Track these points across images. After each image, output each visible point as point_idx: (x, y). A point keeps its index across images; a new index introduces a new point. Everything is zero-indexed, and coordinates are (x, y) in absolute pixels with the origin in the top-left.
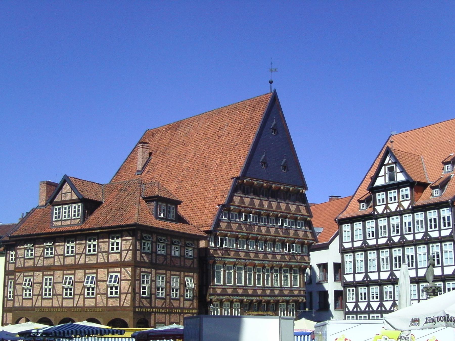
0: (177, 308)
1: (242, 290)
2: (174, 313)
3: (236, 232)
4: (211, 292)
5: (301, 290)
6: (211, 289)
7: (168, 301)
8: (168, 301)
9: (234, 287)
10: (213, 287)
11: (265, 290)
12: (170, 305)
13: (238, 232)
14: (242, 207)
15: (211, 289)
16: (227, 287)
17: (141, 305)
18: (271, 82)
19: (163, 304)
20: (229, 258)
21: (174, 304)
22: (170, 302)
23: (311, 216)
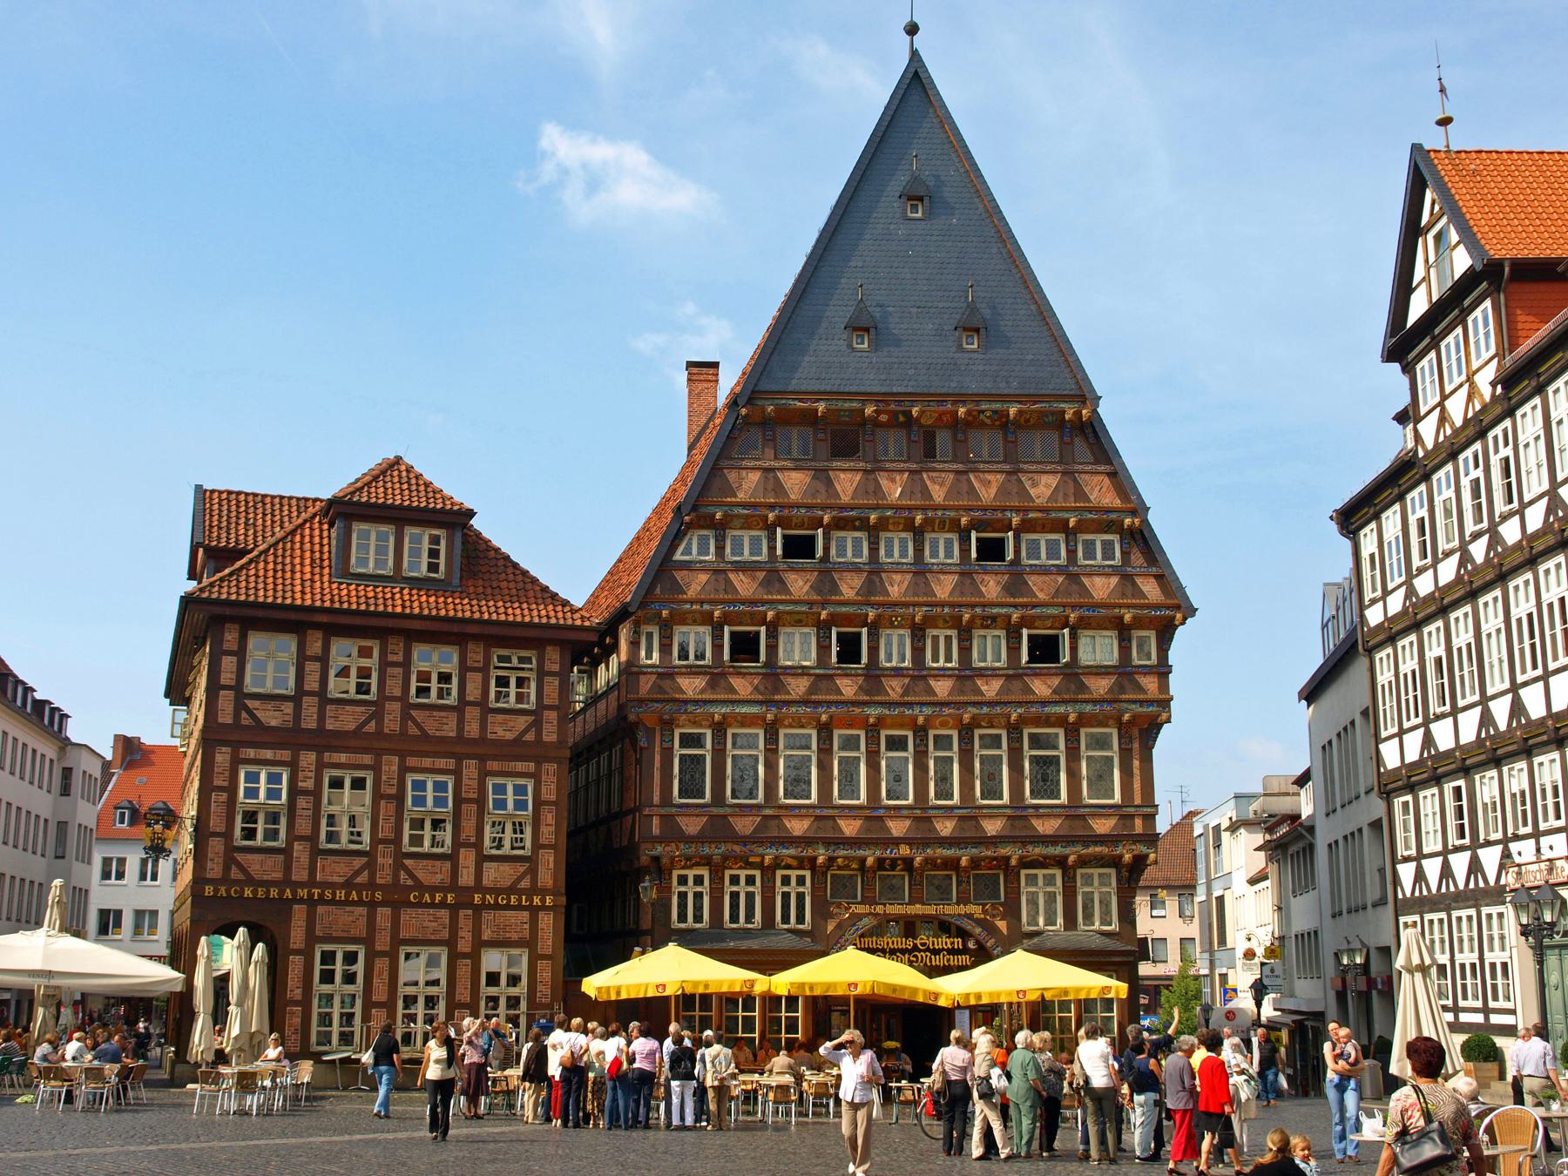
0: (433, 889)
1: (806, 823)
2: (420, 904)
3: (753, 602)
4: (656, 831)
5: (1132, 817)
6: (656, 821)
7: (385, 860)
8: (385, 860)
9: (768, 812)
10: (663, 811)
11: (929, 819)
12: (396, 876)
13: (764, 603)
14: (772, 507)
15: (656, 821)
16: (728, 810)
17: (235, 873)
18: (912, 29)
19: (357, 873)
20: (733, 702)
21: (420, 875)
22: (398, 866)
23: (1140, 509)
